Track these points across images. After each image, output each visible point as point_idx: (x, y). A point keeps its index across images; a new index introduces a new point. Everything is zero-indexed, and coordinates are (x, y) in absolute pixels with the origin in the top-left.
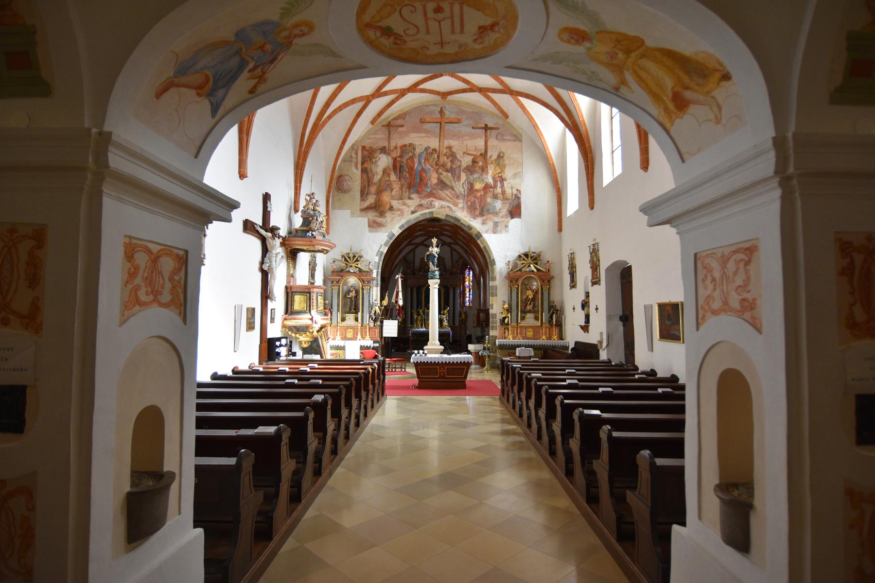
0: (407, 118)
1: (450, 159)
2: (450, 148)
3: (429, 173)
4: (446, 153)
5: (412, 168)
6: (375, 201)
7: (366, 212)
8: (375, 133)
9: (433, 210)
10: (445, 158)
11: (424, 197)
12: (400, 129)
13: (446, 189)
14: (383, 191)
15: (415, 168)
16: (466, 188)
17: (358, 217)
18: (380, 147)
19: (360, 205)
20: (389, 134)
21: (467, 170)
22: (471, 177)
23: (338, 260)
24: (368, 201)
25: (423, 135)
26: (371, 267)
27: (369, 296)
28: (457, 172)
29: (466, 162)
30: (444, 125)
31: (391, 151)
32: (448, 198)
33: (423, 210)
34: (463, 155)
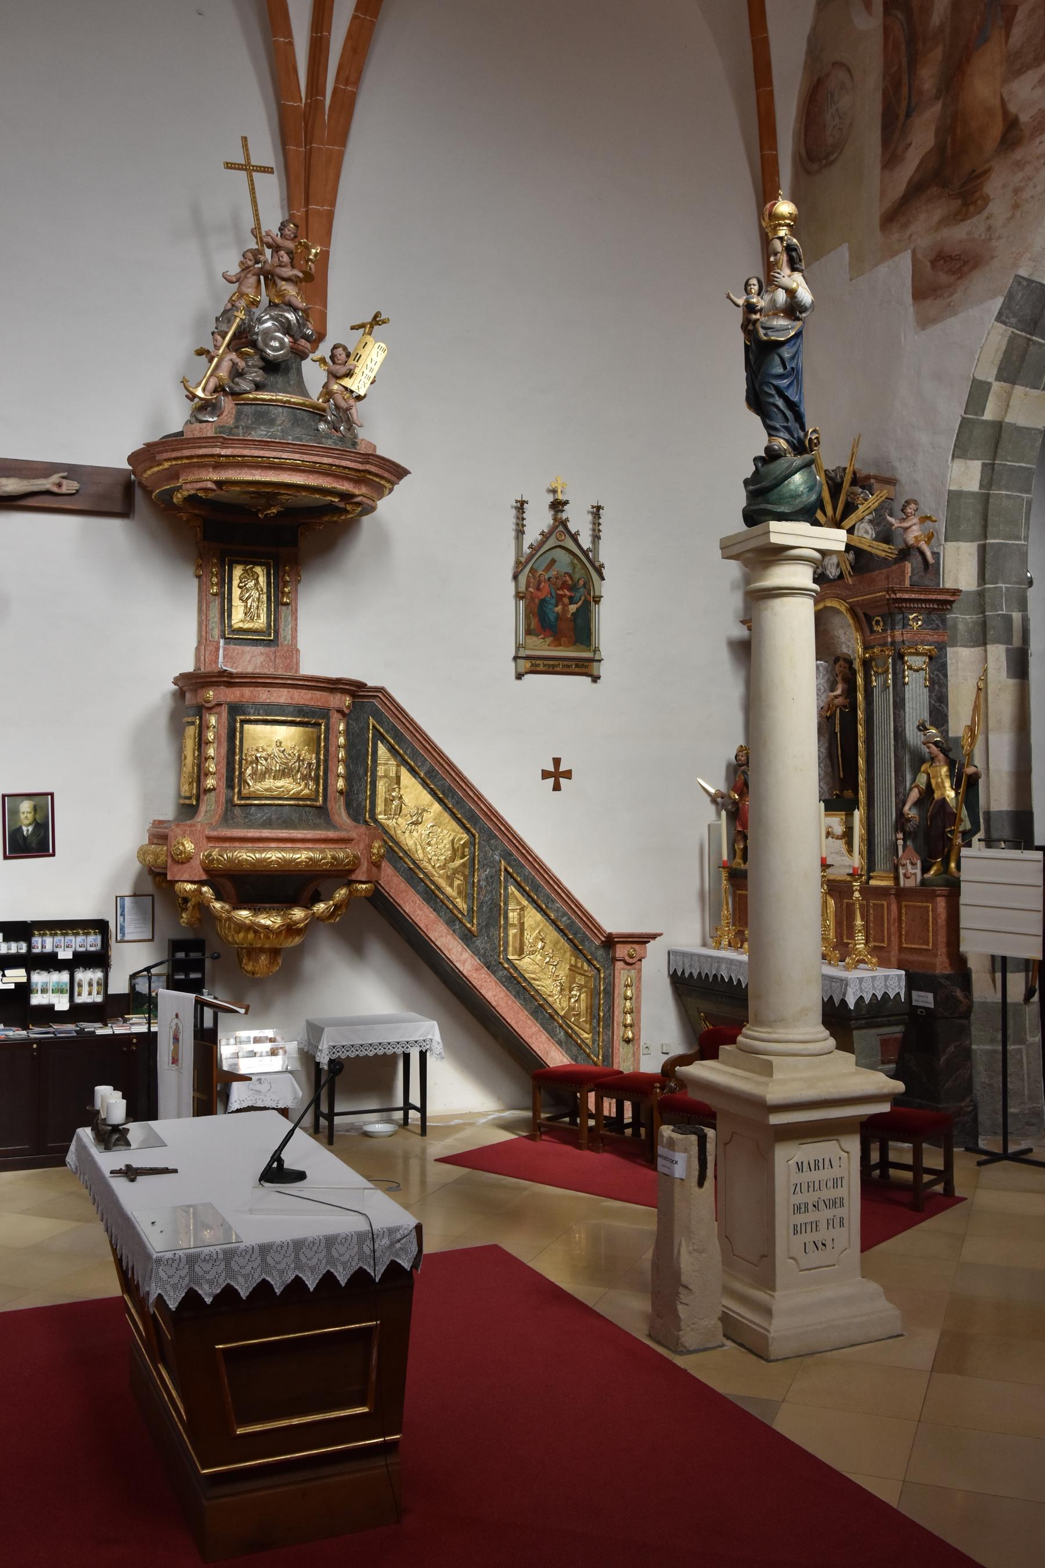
6: (936, 136)
17: (875, 266)
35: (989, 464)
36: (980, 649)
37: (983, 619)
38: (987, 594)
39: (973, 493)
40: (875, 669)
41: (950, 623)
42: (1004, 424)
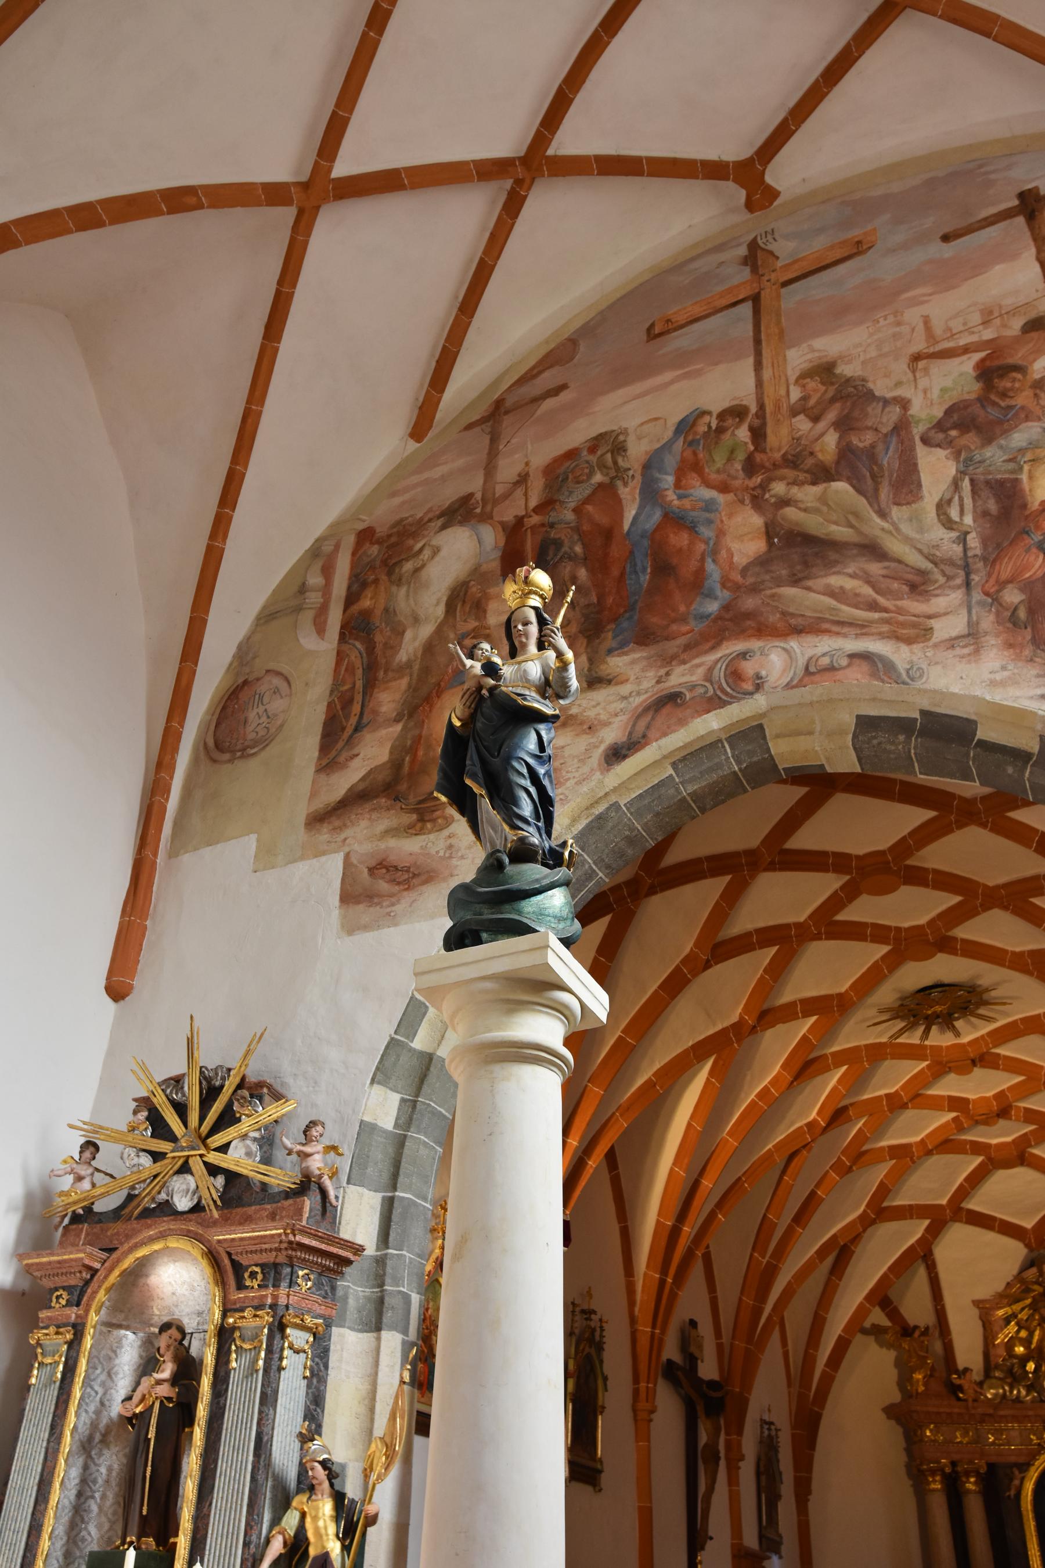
0: (582, 347)
1: (831, 415)
2: (825, 370)
3: (710, 522)
4: (804, 399)
5: (608, 534)
6: (391, 753)
7: (337, 823)
8: (431, 461)
9: (759, 702)
10: (803, 424)
11: (687, 647)
12: (549, 404)
13: (830, 566)
14: (438, 697)
15: (626, 526)
16: (968, 520)
17: (295, 861)
18: (447, 505)
19: (313, 794)
20: (494, 439)
21: (955, 426)
22: (989, 452)
23: (115, 1137)
24: (356, 763)
25: (668, 376)
26: (316, 1163)
27: (269, 1399)
28: (888, 459)
29: (935, 393)
30: (778, 297)
31: (496, 502)
32: (848, 611)
33: (682, 722)
34: (914, 372)
35: (409, 1100)
36: (370, 1336)
37: (379, 1294)
38: (389, 1263)
39: (385, 1131)
40: (238, 1343)
41: (340, 1293)
42: (435, 1057)
